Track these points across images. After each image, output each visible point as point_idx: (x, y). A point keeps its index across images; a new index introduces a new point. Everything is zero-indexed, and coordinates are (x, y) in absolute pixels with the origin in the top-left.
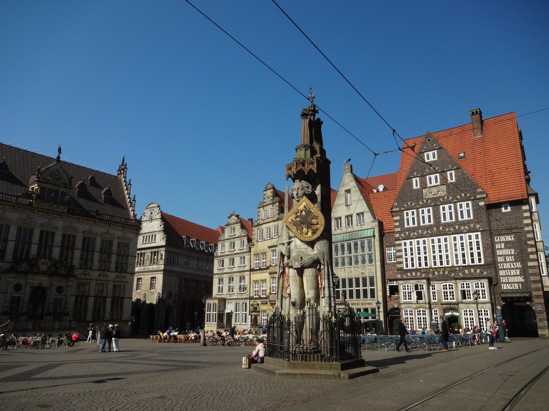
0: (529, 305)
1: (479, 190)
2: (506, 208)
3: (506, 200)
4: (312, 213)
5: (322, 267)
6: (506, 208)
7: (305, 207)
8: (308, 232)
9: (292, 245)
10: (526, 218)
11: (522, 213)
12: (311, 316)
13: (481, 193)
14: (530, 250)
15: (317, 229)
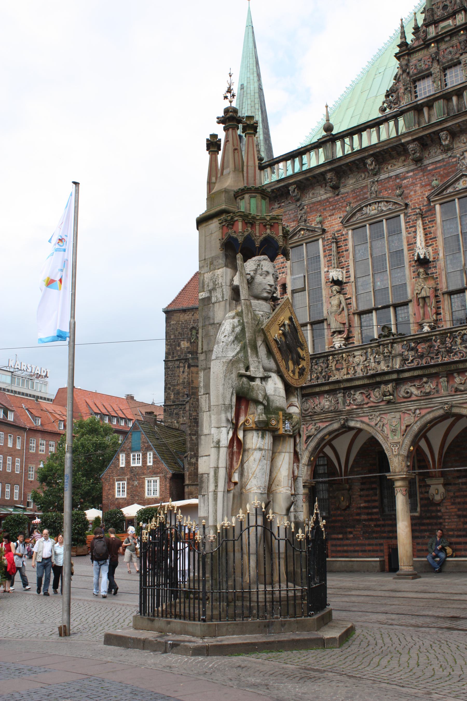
7: (290, 319)
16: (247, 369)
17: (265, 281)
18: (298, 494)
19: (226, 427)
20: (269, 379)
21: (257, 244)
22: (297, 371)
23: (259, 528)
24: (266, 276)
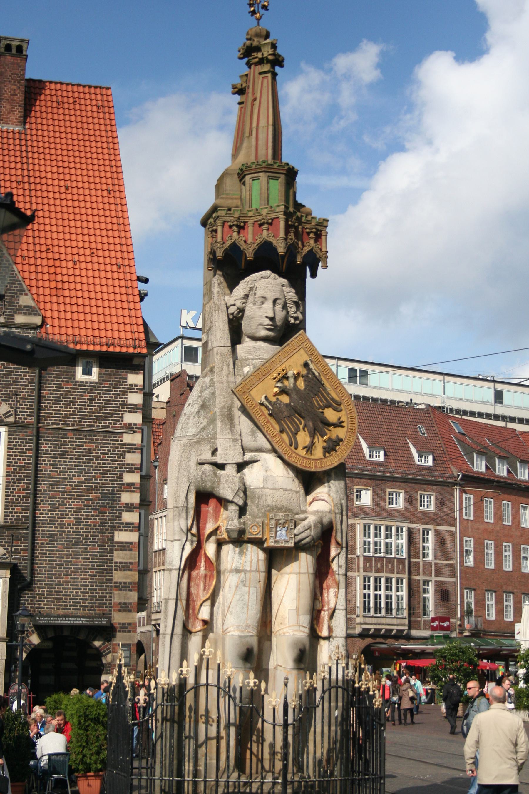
0: (97, 649)
1: (25, 300)
2: (87, 372)
3: (91, 348)
4: (325, 389)
5: (333, 552)
6: (87, 372)
7: (306, 365)
8: (313, 444)
9: (253, 476)
10: (132, 408)
11: (124, 394)
12: (333, 691)
13: (29, 310)
14: (126, 498)
15: (339, 441)
16: (214, 452)
17: (259, 313)
18: (336, 637)
19: (179, 540)
20: (256, 464)
21: (250, 256)
22: (320, 444)
23: (340, 690)
24: (263, 303)
